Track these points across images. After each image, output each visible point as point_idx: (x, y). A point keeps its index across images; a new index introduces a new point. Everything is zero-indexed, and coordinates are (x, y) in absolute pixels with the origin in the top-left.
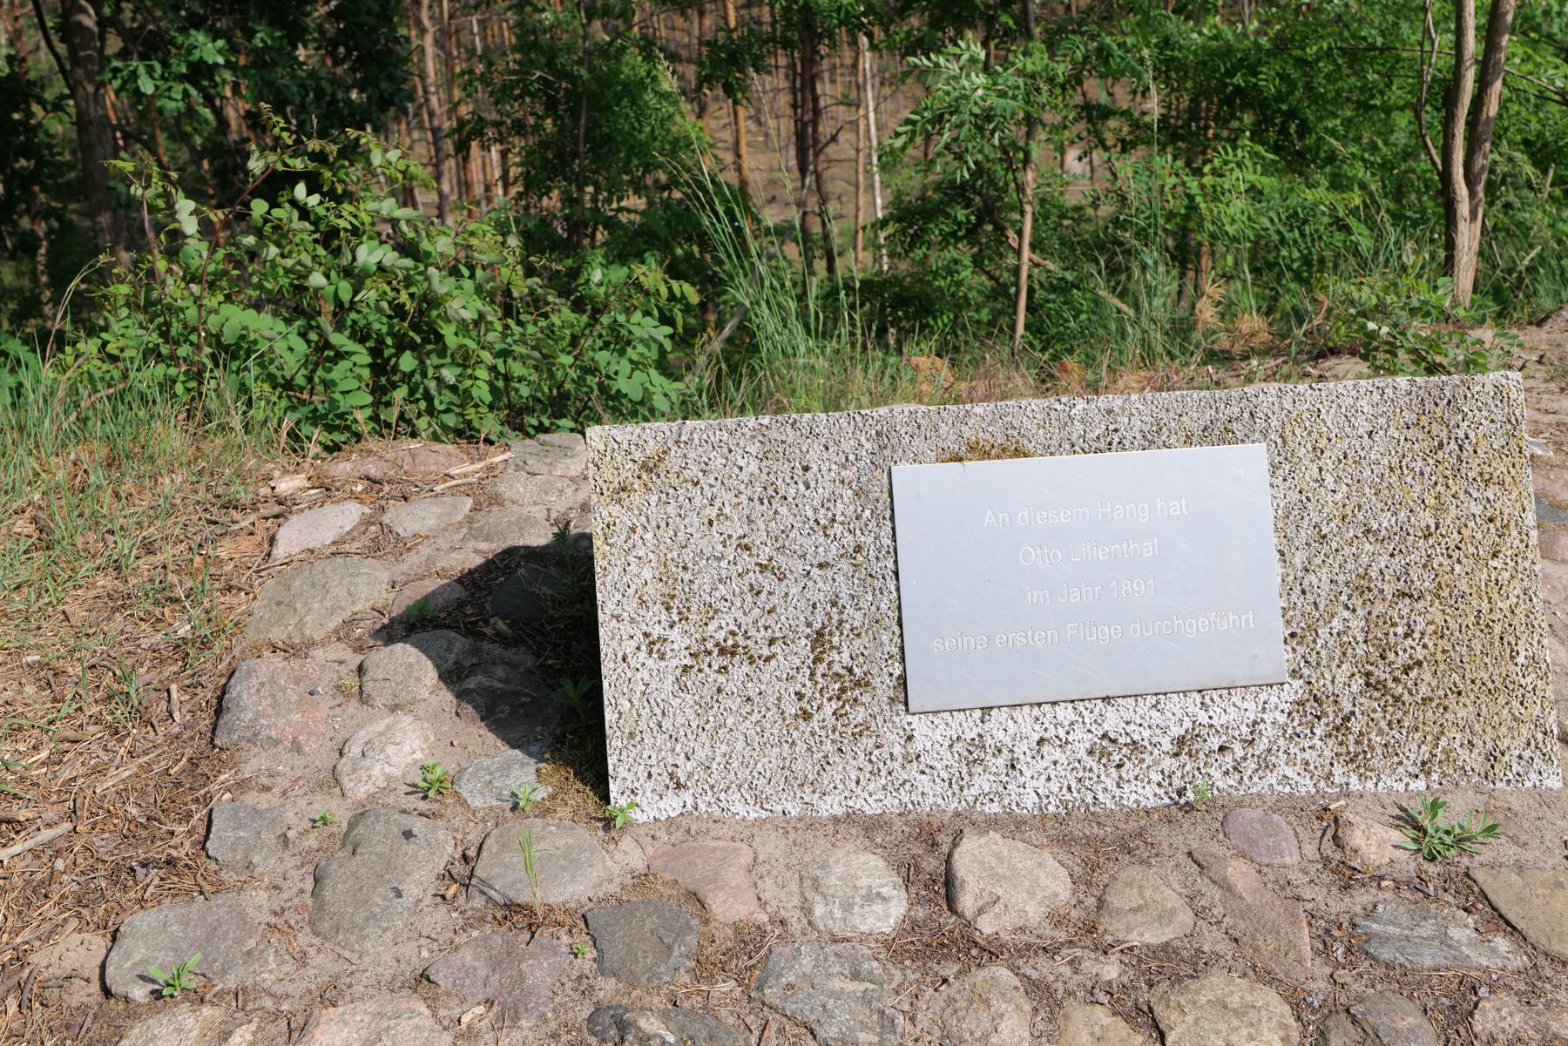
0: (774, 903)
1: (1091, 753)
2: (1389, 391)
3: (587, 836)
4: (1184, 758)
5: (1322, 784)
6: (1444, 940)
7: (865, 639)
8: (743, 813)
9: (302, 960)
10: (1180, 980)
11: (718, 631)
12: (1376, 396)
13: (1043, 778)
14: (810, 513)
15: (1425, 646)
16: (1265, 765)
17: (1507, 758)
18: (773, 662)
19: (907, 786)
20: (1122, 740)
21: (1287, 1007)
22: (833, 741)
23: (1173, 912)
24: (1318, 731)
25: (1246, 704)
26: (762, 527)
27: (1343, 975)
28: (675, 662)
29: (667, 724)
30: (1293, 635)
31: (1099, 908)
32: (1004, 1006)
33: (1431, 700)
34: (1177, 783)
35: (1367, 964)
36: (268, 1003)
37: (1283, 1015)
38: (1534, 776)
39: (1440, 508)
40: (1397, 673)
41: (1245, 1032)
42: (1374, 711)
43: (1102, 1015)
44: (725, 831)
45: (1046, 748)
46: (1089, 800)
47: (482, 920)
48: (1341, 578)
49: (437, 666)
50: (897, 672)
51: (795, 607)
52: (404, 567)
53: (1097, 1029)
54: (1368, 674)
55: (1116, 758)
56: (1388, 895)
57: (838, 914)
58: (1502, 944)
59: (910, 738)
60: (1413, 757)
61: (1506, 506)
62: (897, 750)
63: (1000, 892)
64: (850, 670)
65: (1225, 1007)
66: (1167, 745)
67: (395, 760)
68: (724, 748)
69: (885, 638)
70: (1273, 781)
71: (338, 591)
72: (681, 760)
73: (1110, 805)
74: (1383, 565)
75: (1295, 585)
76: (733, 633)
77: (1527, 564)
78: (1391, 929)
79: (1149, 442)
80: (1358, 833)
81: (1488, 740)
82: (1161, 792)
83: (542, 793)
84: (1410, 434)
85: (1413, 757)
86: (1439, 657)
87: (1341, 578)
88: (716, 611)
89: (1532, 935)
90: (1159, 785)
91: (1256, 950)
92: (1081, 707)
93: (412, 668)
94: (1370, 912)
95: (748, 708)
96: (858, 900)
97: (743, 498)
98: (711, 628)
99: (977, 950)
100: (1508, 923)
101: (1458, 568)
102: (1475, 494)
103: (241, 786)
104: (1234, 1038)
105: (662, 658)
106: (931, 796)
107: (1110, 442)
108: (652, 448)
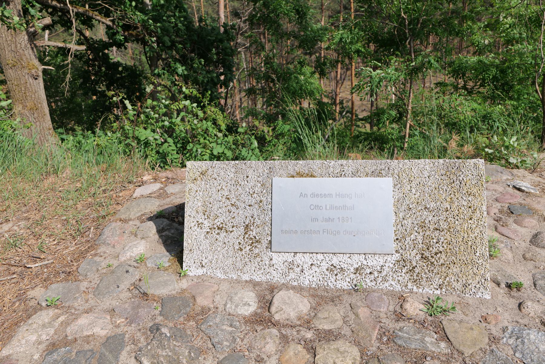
0: (217, 302)
1: (327, 270)
2: (436, 163)
3: (174, 277)
4: (358, 275)
5: (404, 288)
6: (423, 341)
7: (260, 228)
8: (220, 276)
9: (87, 301)
10: (329, 340)
12: (432, 165)
13: (311, 276)
14: (248, 190)
15: (443, 247)
16: (385, 280)
17: (470, 286)
18: (233, 233)
19: (269, 274)
20: (338, 267)
21: (359, 354)
22: (248, 258)
23: (337, 320)
24: (404, 271)
25: (379, 260)
26: (233, 193)
27: (383, 347)
28: (205, 230)
29: (201, 248)
30: (397, 239)
31: (314, 316)
32: (270, 340)
33: (444, 264)
34: (355, 282)
35: (392, 344)
36: (73, 311)
37: (356, 356)
38: (480, 294)
39: (452, 202)
40: (433, 255)
41: (341, 359)
42: (424, 266)
43: (300, 348)
44: (214, 281)
45: (313, 267)
46: (326, 284)
47: (136, 297)
48: (415, 222)
49: (157, 228)
50: (269, 239)
51: (241, 216)
52: (164, 202)
53: (297, 351)
54: (423, 254)
55: (335, 272)
56: (411, 325)
57: (233, 307)
58: (443, 345)
59: (271, 259)
60: (436, 283)
61: (476, 203)
62: (267, 263)
63: (284, 307)
64: (255, 237)
65: (338, 351)
66: (352, 270)
67: (134, 252)
68: (216, 257)
69: (266, 229)
70: (387, 285)
71: (142, 206)
72: (204, 259)
73: (332, 287)
74: (430, 219)
75: (399, 223)
76: (222, 223)
77: (482, 223)
78: (405, 335)
79: (354, 175)
80: (409, 304)
81: (464, 280)
82: (349, 285)
83: (167, 265)
84: (442, 178)
85: (436, 283)
86: (448, 250)
87: (415, 222)
88: (218, 217)
89: (454, 343)
90: (349, 282)
91: (358, 335)
92: (325, 255)
93: (151, 228)
94: (401, 330)
95: (224, 246)
96: (241, 304)
97: (229, 184)
98: (216, 221)
99: (270, 322)
100: (448, 339)
101: (457, 222)
102: (465, 198)
103: (96, 255)
104: (336, 360)
105: (201, 229)
106: (276, 277)
107: (341, 175)
108: (204, 168)
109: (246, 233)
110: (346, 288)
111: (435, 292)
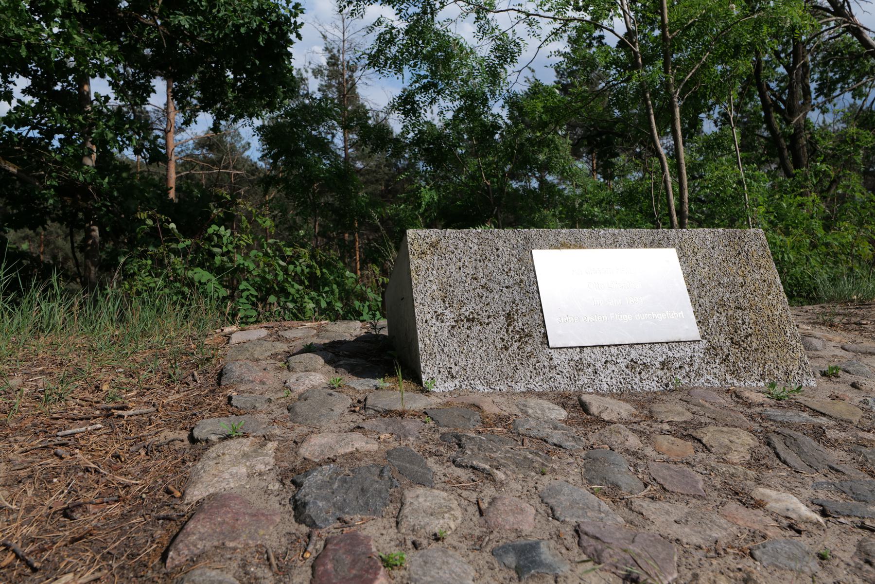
1: (627, 367)
7: (528, 317)
11: (466, 311)
12: (712, 234)
16: (699, 375)
24: (717, 361)
28: (448, 324)
29: (446, 350)
39: (744, 276)
45: (608, 365)
46: (630, 387)
50: (543, 331)
51: (498, 301)
54: (732, 339)
62: (546, 364)
64: (523, 330)
66: (658, 365)
68: (471, 361)
72: (453, 366)
76: (472, 313)
84: (728, 248)
89: (834, 415)
98: (463, 310)
108: (434, 238)
109: (509, 325)
110: (655, 389)
111: (759, 385)
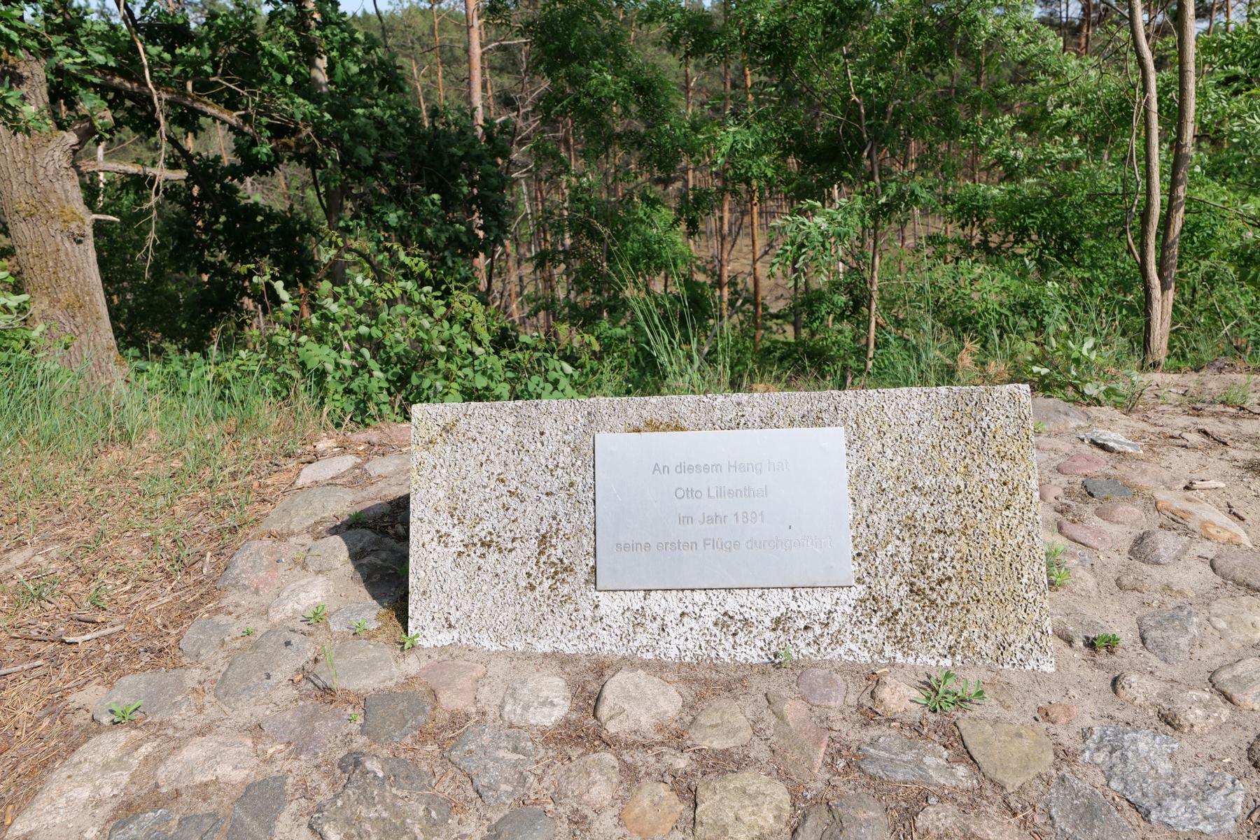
1: (716, 624)
2: (933, 395)
3: (390, 652)
4: (779, 632)
5: (876, 656)
6: (919, 764)
7: (572, 542)
9: (201, 710)
10: (725, 772)
11: (481, 532)
12: (924, 398)
13: (683, 639)
14: (543, 461)
15: (954, 567)
16: (836, 641)
17: (1012, 648)
20: (738, 617)
21: (788, 797)
23: (739, 729)
24: (875, 621)
25: (824, 599)
27: (837, 780)
28: (454, 549)
30: (859, 555)
33: (957, 604)
34: (774, 648)
36: (170, 732)
38: (1033, 663)
39: (968, 474)
40: (933, 585)
41: (750, 809)
42: (916, 609)
43: (663, 790)
44: (475, 657)
45: (686, 619)
46: (713, 655)
47: (309, 696)
48: (895, 518)
49: (349, 550)
50: (591, 564)
51: (530, 517)
52: (364, 494)
53: (656, 798)
54: (912, 584)
55: (733, 629)
57: (519, 711)
58: (961, 770)
59: (597, 607)
60: (943, 643)
61: (1016, 474)
63: (626, 706)
64: (561, 561)
65: (744, 792)
66: (768, 623)
67: (303, 601)
68: (479, 604)
69: (585, 542)
70: (842, 652)
71: (317, 504)
72: (453, 611)
73: (727, 660)
74: (925, 511)
75: (862, 521)
76: (490, 533)
77: (1031, 515)
79: (765, 423)
80: (887, 689)
81: (999, 634)
82: (763, 654)
83: (373, 626)
84: (947, 424)
85: (943, 643)
86: (964, 575)
87: (895, 518)
89: (984, 767)
91: (784, 758)
92: (710, 593)
93: (338, 549)
98: (477, 529)
100: (971, 757)
101: (979, 515)
102: (993, 466)
103: (217, 611)
104: (741, 812)
106: (608, 644)
108: (449, 418)
109: (541, 553)
110: (756, 660)
111: (942, 663)
